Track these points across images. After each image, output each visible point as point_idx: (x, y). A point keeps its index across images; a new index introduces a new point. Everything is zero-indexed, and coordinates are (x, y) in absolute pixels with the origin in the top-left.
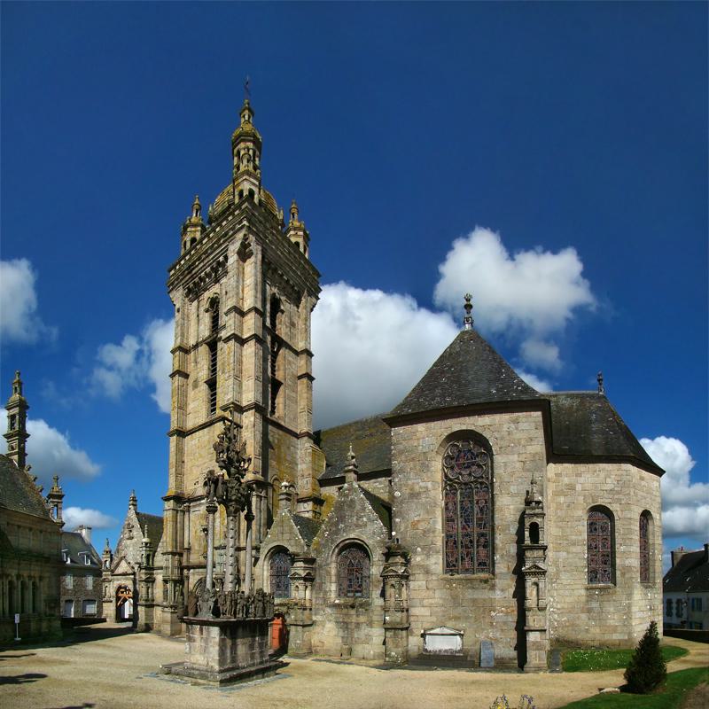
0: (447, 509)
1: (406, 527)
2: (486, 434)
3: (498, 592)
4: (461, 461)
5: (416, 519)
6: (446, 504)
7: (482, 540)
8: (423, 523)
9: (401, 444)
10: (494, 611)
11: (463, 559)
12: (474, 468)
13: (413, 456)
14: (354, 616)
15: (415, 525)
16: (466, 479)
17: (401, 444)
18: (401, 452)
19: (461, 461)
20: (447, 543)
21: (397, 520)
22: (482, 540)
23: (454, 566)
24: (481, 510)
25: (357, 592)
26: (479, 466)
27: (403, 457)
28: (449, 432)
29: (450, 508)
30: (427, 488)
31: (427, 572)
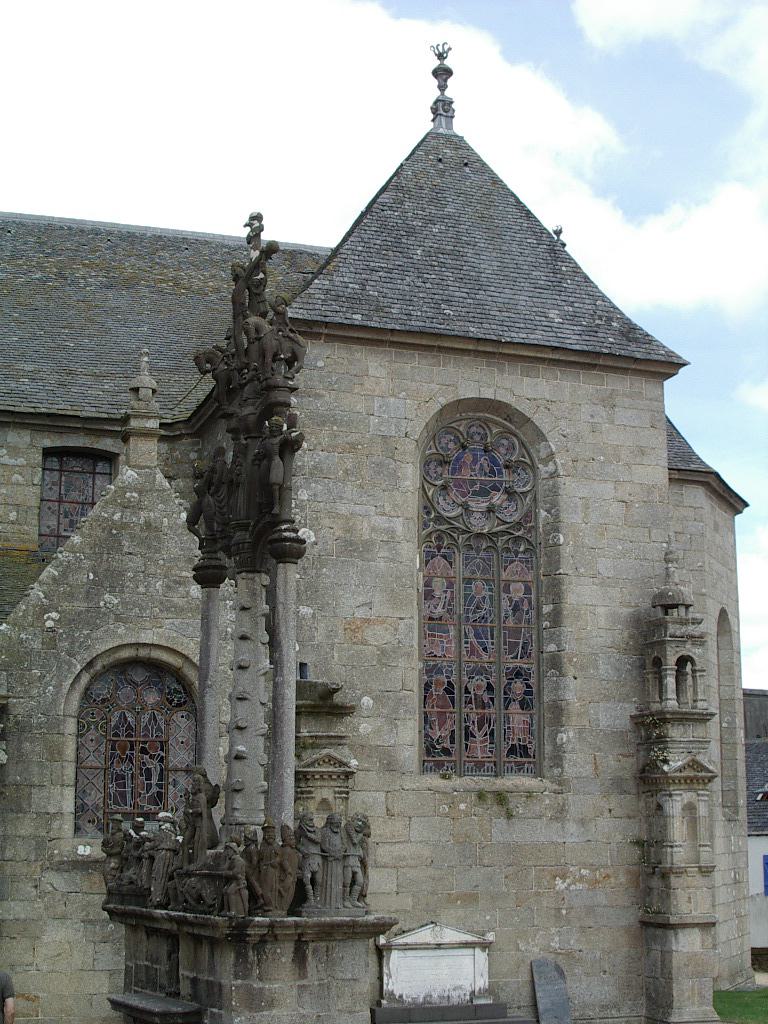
0: (428, 595)
1: (331, 634)
2: (541, 420)
3: (572, 827)
4: (466, 474)
5: (360, 613)
6: (427, 584)
7: (518, 686)
8: (379, 629)
9: (318, 396)
10: (564, 877)
11: (469, 735)
12: (498, 498)
15: (354, 628)
16: (480, 524)
17: (318, 396)
18: (323, 421)
19: (466, 474)
20: (427, 686)
22: (518, 686)
23: (446, 752)
24: (516, 608)
26: (510, 494)
28: (451, 398)
29: (437, 593)
30: (391, 532)
31: (390, 765)
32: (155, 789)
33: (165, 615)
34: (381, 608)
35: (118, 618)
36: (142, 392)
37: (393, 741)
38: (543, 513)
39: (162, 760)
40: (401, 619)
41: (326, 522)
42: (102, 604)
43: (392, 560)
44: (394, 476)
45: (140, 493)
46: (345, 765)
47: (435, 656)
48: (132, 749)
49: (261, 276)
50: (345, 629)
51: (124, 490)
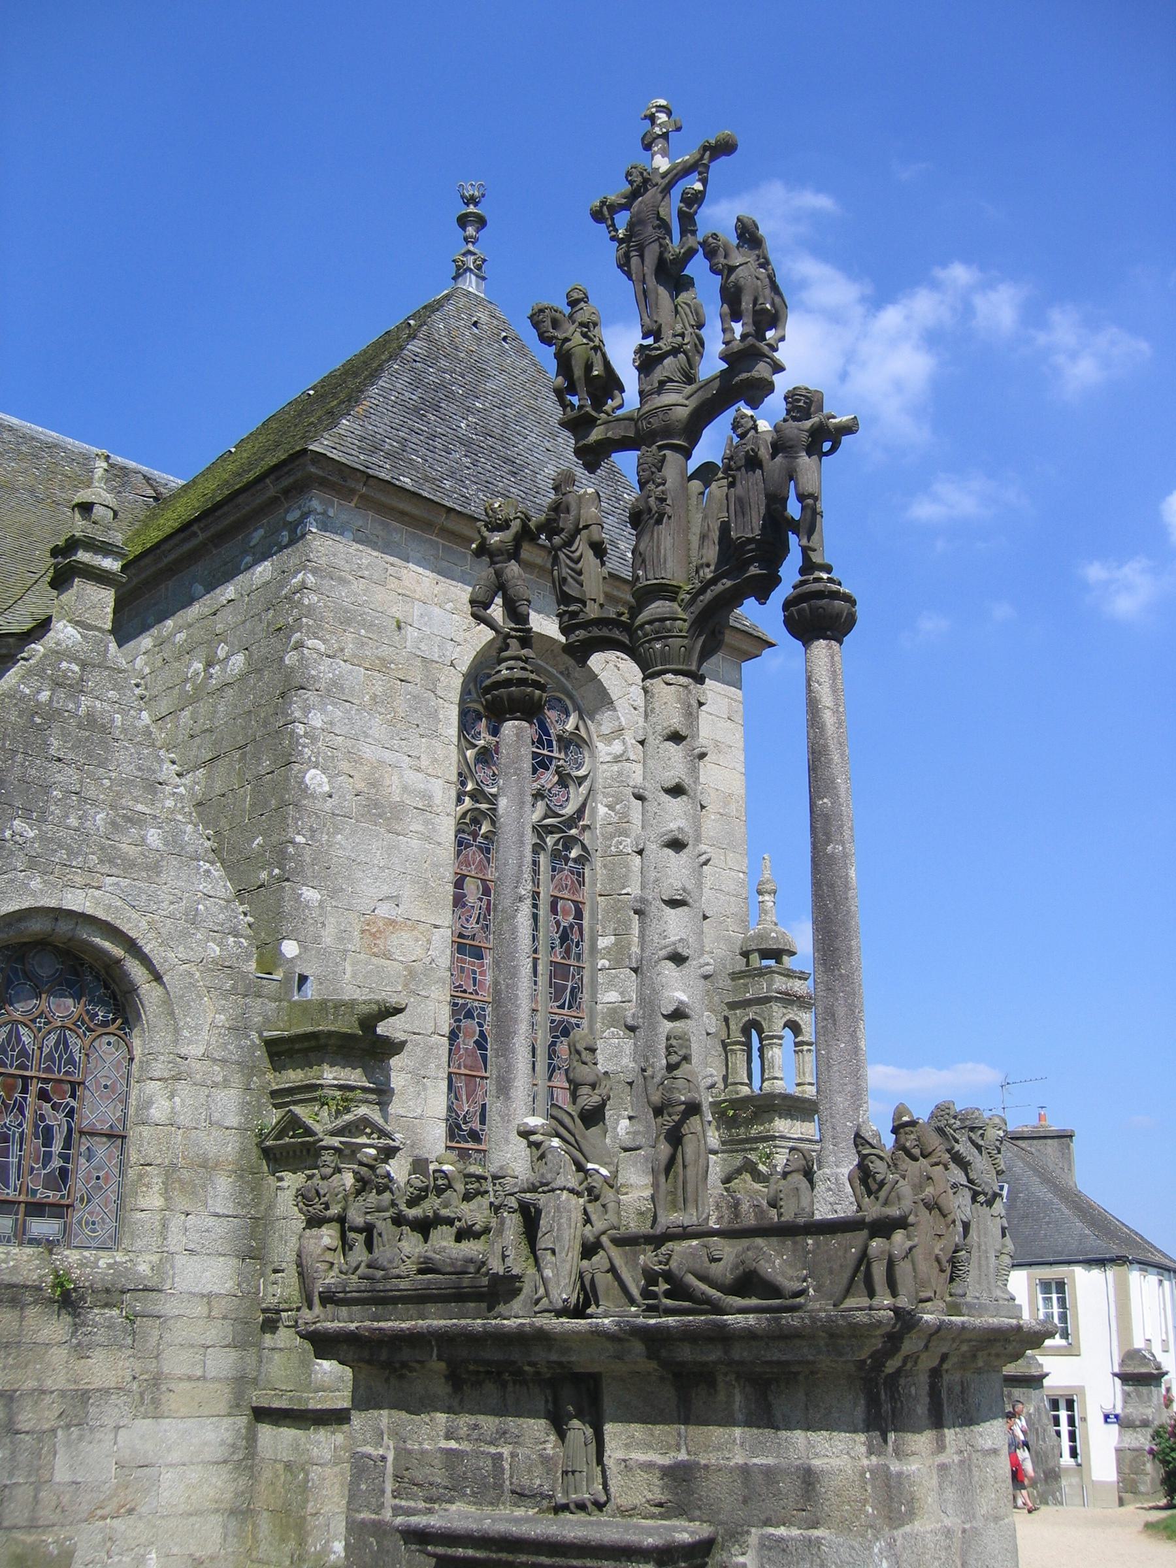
1: (342, 936)
5: (384, 910)
9: (342, 581)
13: (385, 651)
14: (59, 1355)
17: (342, 581)
18: (347, 619)
21: (310, 894)
25: (37, 1209)
27: (349, 641)
30: (427, 796)
32: (56, 1163)
33: (105, 869)
34: (411, 908)
35: (33, 863)
36: (98, 511)
37: (419, 1111)
38: (602, 810)
39: (71, 1113)
40: (436, 927)
41: (344, 766)
42: (8, 834)
43: (428, 839)
44: (434, 715)
45: (83, 665)
46: (388, 1135)
47: (465, 991)
48: (25, 1090)
49: (698, 186)
50: (363, 931)
51: (58, 654)
